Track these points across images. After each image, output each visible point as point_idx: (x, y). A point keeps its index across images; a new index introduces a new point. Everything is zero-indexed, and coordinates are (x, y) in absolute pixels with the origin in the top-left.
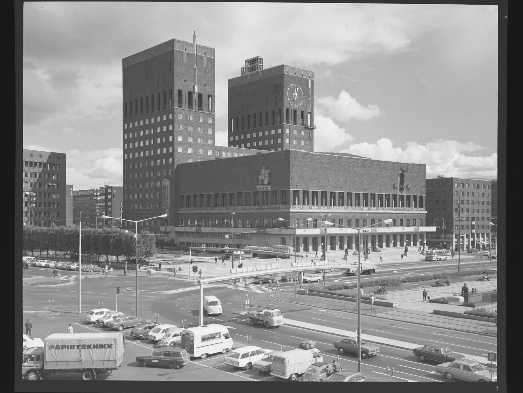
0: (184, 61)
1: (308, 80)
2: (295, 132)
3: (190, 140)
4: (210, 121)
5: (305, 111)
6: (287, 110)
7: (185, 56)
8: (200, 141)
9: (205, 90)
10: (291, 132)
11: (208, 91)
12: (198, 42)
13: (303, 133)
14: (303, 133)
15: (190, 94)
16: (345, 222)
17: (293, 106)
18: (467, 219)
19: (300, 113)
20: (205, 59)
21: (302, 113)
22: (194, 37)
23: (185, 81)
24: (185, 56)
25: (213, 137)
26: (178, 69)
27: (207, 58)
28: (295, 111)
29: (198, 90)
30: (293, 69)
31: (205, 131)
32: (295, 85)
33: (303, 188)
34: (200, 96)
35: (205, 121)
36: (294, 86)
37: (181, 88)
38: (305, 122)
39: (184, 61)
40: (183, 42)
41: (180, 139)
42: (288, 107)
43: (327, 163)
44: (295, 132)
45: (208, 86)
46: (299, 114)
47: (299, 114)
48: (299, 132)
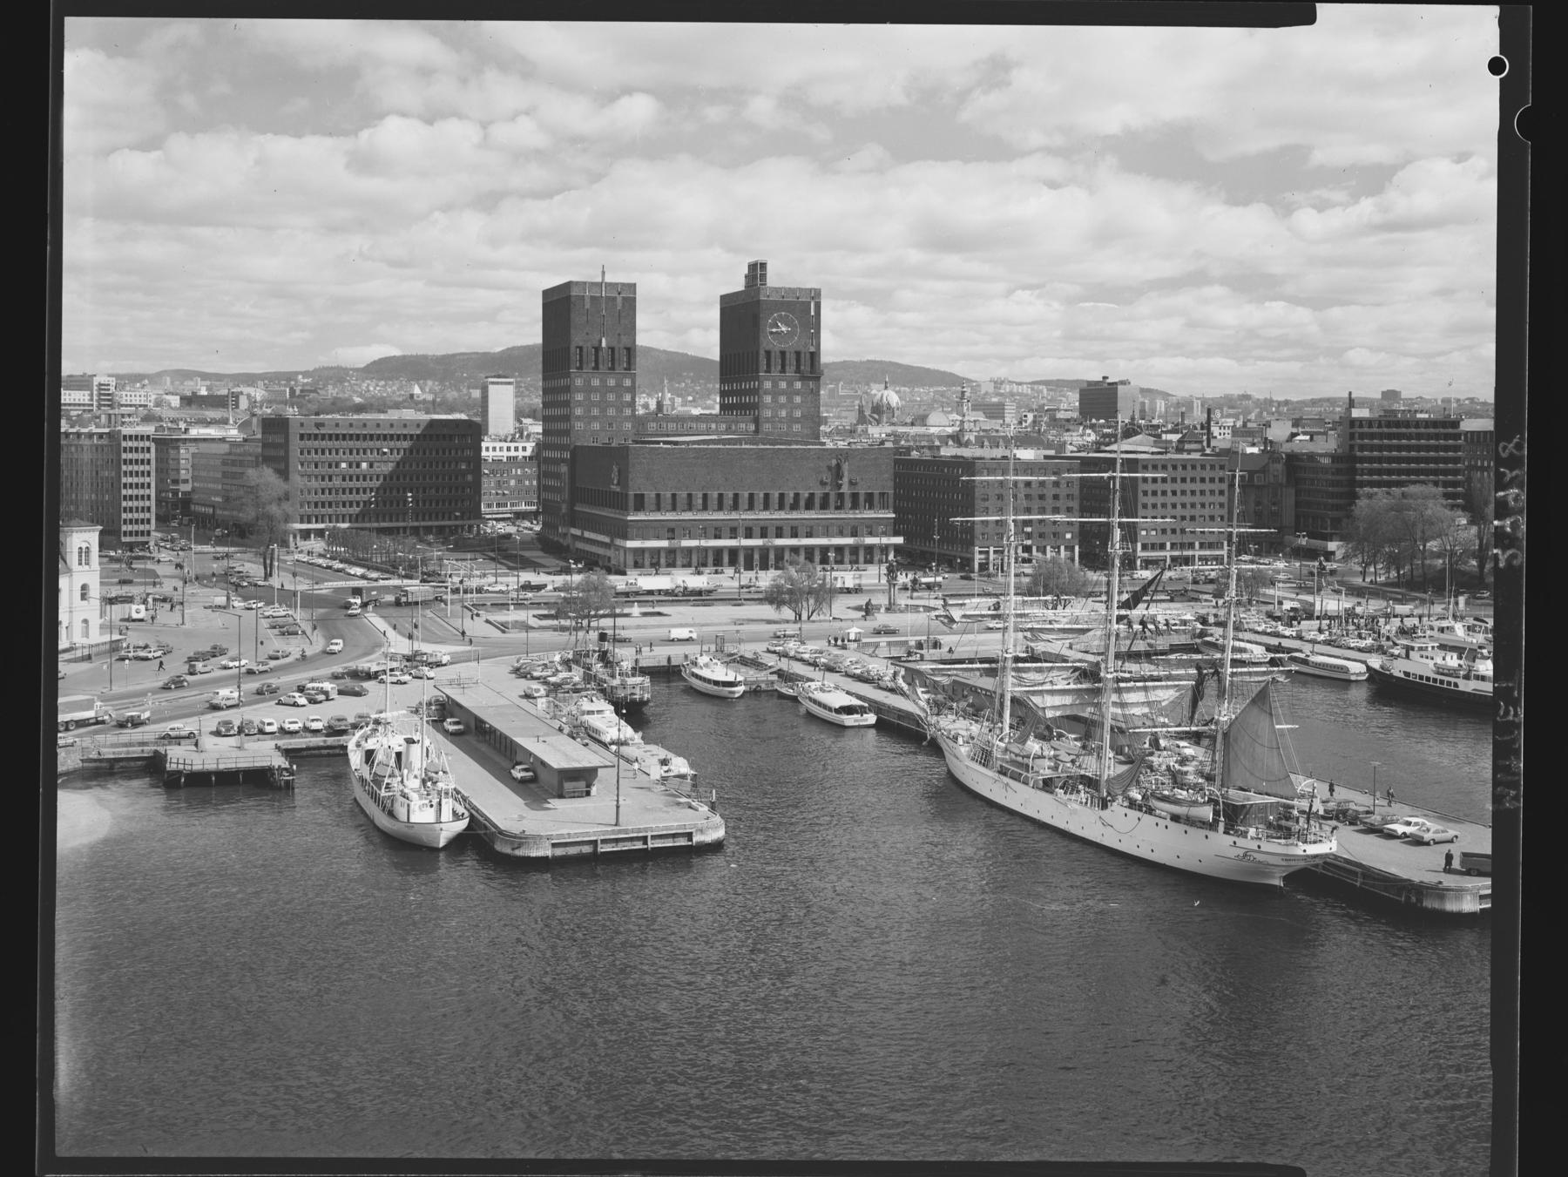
2: (783, 385)
3: (595, 412)
4: (628, 383)
6: (768, 353)
7: (587, 300)
10: (775, 385)
11: (625, 340)
12: (608, 279)
16: (741, 531)
17: (776, 346)
18: (1174, 506)
20: (619, 300)
24: (587, 300)
25: (632, 404)
26: (577, 319)
28: (783, 353)
31: (619, 396)
35: (619, 385)
41: (578, 412)
42: (769, 347)
46: (791, 358)
47: (791, 358)
48: (790, 384)
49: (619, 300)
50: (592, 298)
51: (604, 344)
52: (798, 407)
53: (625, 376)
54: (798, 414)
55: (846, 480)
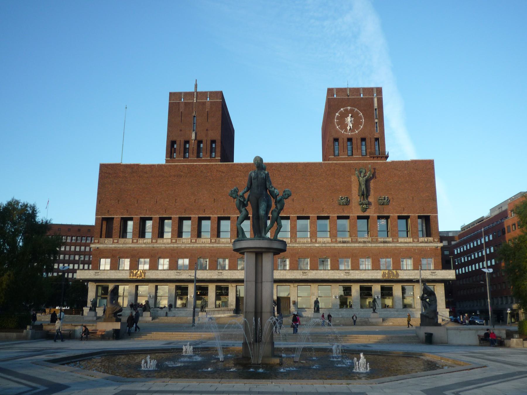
0: (181, 111)
1: (372, 99)
9: (207, 136)
19: (359, 141)
22: (196, 86)
23: (181, 130)
24: (182, 106)
27: (211, 102)
32: (349, 108)
33: (122, 214)
34: (200, 142)
36: (346, 110)
37: (174, 139)
38: (369, 151)
39: (181, 111)
42: (336, 136)
43: (175, 176)
49: (208, 105)
50: (186, 104)
55: (371, 199)
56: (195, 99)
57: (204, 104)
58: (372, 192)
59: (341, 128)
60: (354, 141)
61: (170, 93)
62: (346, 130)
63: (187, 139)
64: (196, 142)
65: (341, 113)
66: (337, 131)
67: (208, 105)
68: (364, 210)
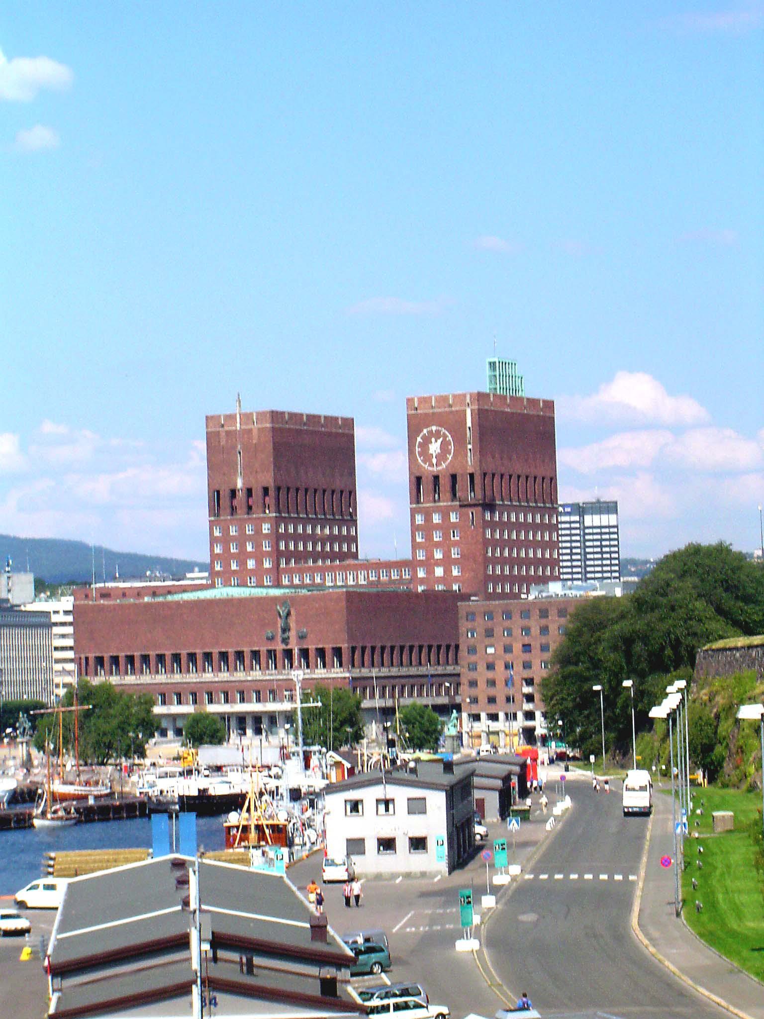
2: (436, 519)
5: (459, 472)
8: (251, 564)
13: (453, 518)
14: (453, 518)
15: (233, 493)
21: (454, 477)
27: (259, 429)
29: (244, 484)
30: (424, 400)
32: (434, 428)
34: (249, 492)
35: (258, 531)
36: (431, 432)
40: (220, 416)
44: (436, 519)
45: (263, 472)
47: (445, 483)
49: (255, 432)
50: (228, 433)
51: (240, 484)
52: (456, 544)
53: (264, 520)
54: (455, 554)
55: (293, 634)
56: (238, 425)
57: (250, 431)
58: (293, 625)
59: (424, 461)
60: (441, 481)
61: (207, 417)
62: (431, 465)
63: (232, 488)
64: (245, 491)
65: (423, 438)
66: (419, 466)
67: (255, 432)
68: (287, 644)
